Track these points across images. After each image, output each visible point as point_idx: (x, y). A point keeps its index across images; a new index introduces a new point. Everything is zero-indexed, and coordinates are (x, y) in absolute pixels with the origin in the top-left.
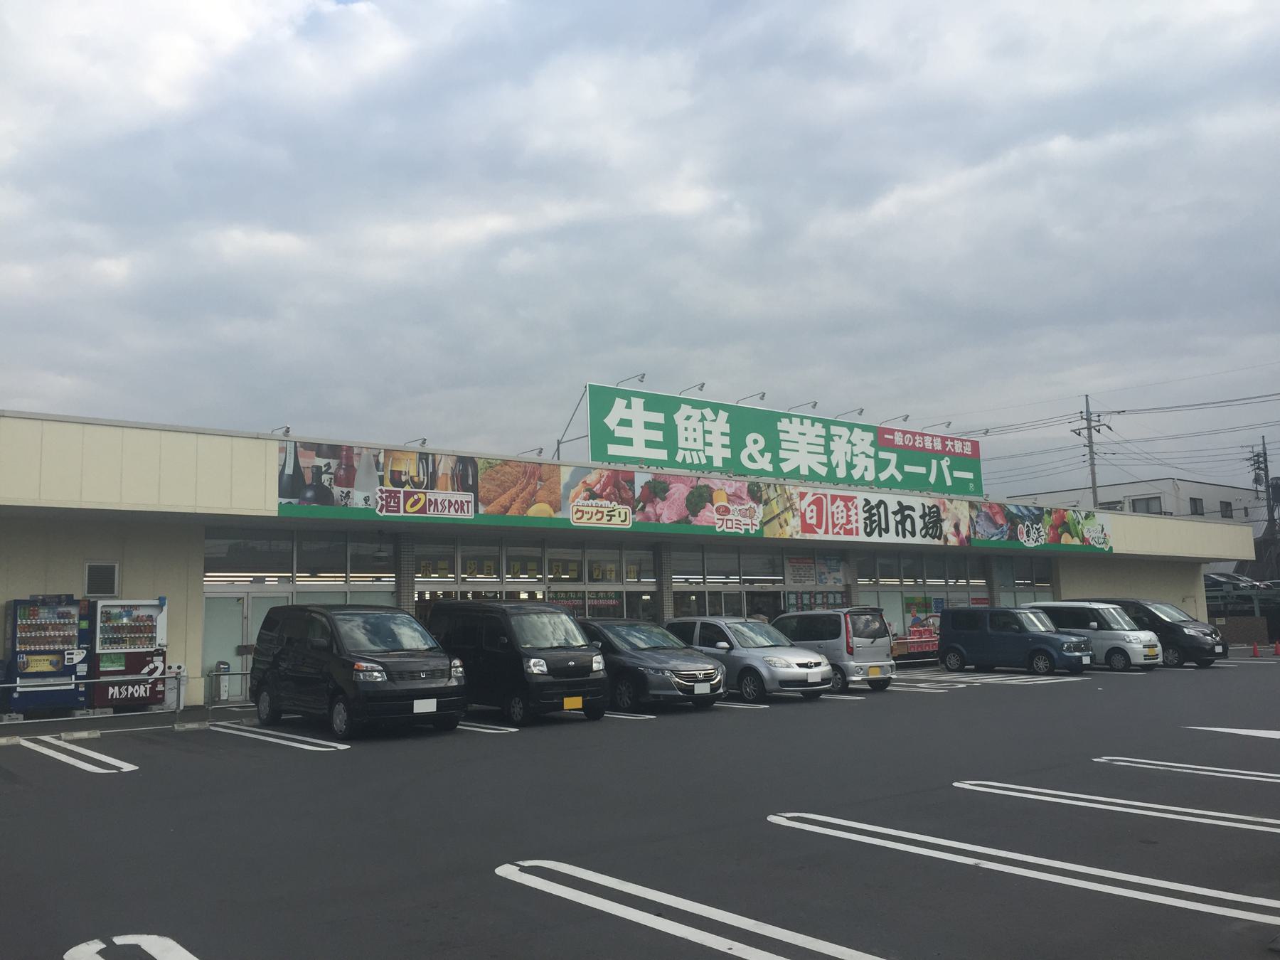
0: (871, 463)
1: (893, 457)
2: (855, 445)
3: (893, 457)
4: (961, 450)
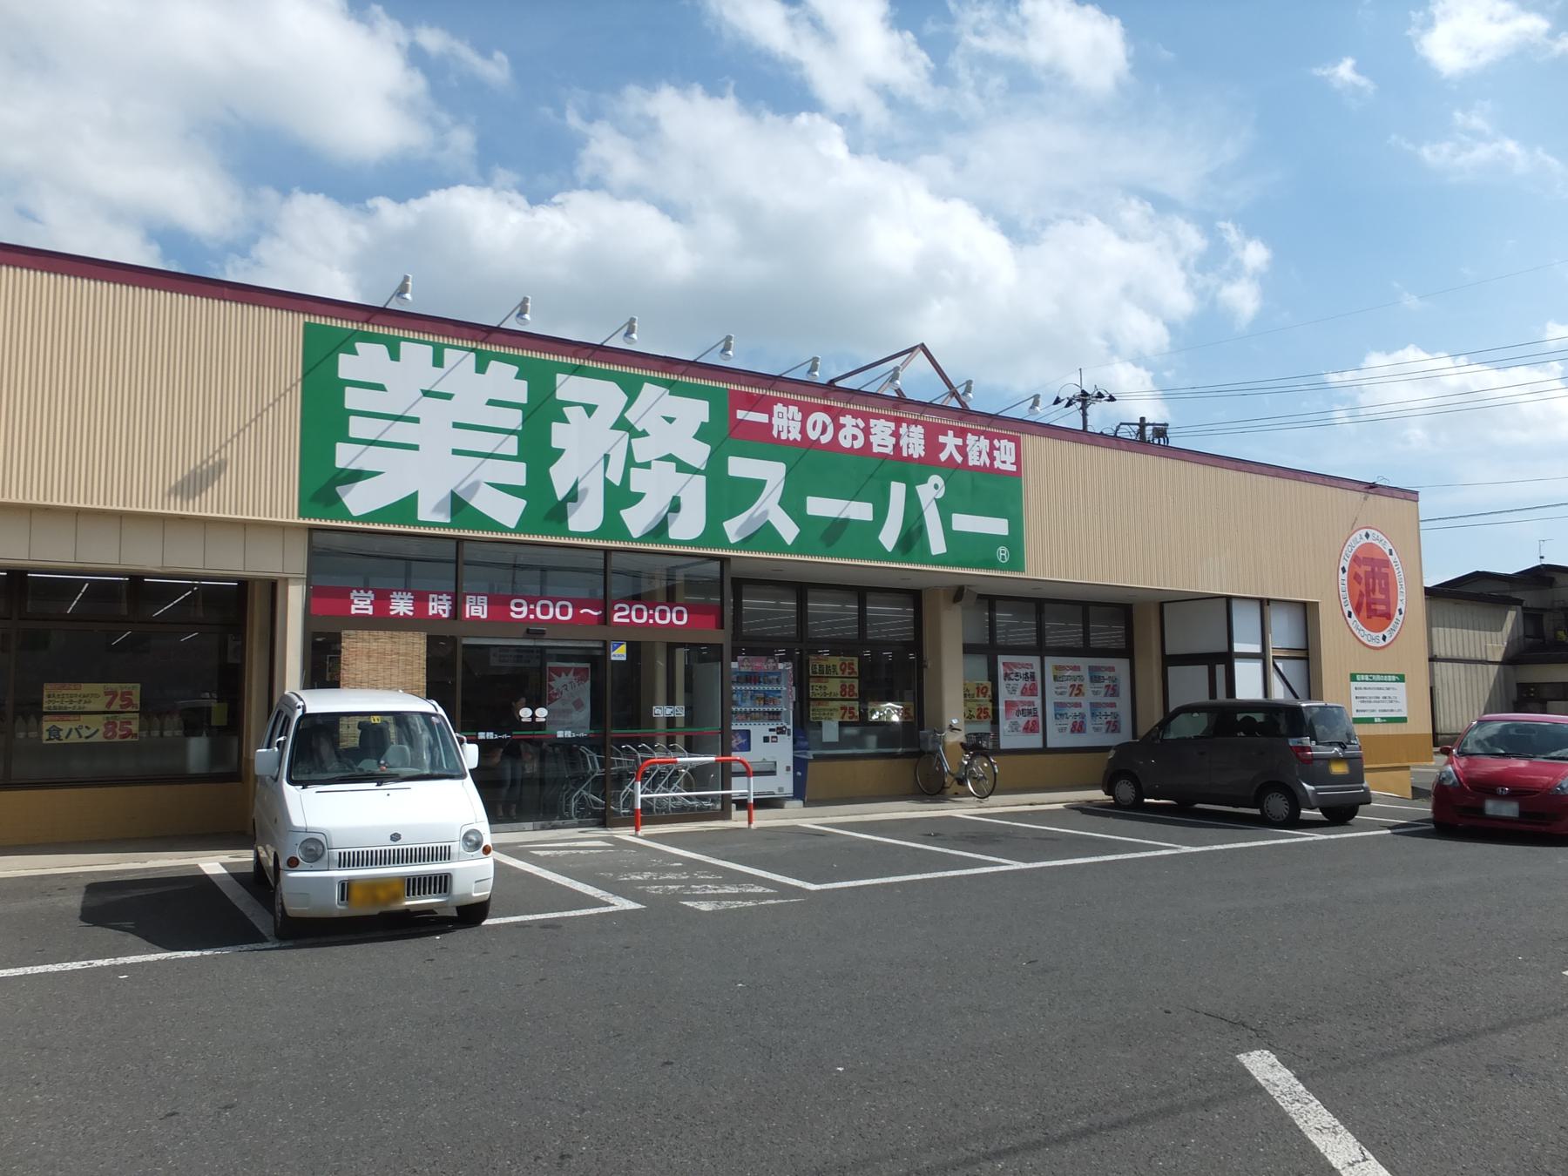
1: (773, 473)
2: (644, 434)
3: (773, 473)
4: (985, 459)
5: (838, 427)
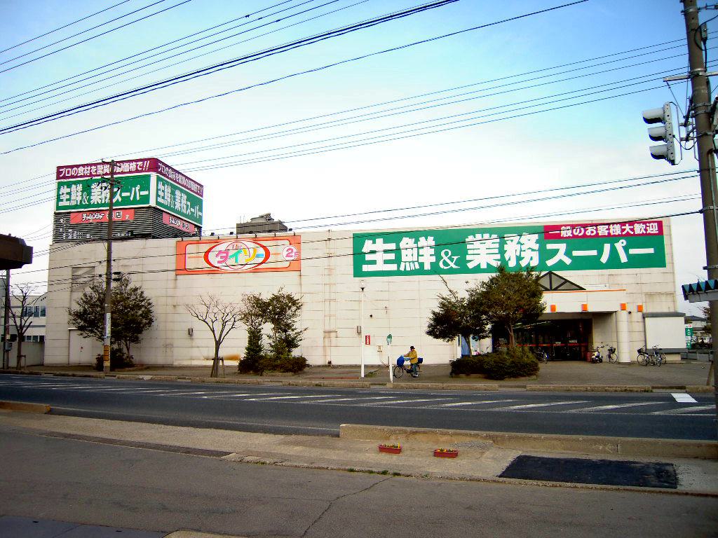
0: (536, 256)
1: (562, 247)
5: (585, 230)
